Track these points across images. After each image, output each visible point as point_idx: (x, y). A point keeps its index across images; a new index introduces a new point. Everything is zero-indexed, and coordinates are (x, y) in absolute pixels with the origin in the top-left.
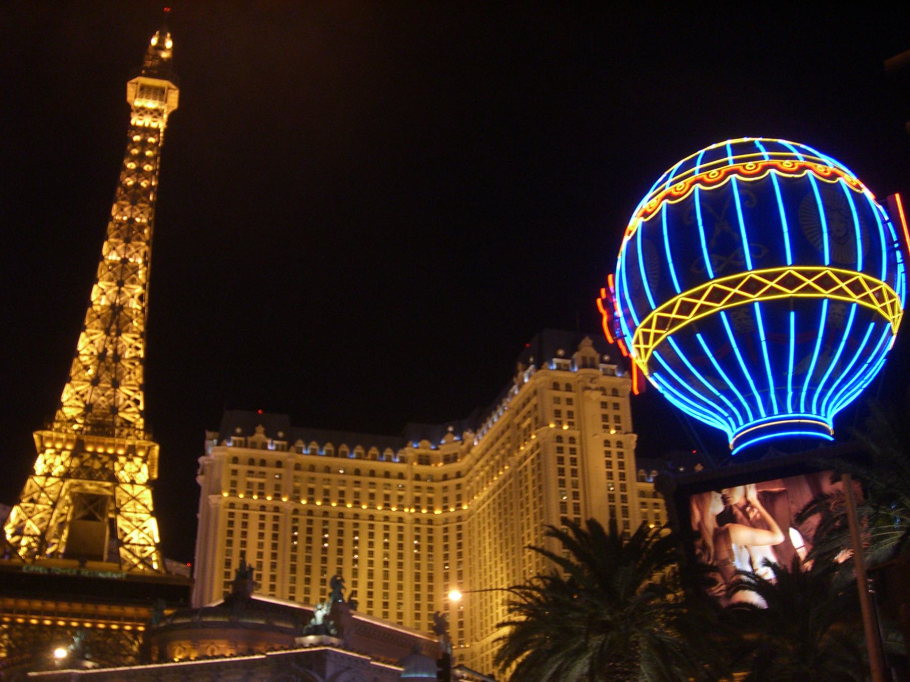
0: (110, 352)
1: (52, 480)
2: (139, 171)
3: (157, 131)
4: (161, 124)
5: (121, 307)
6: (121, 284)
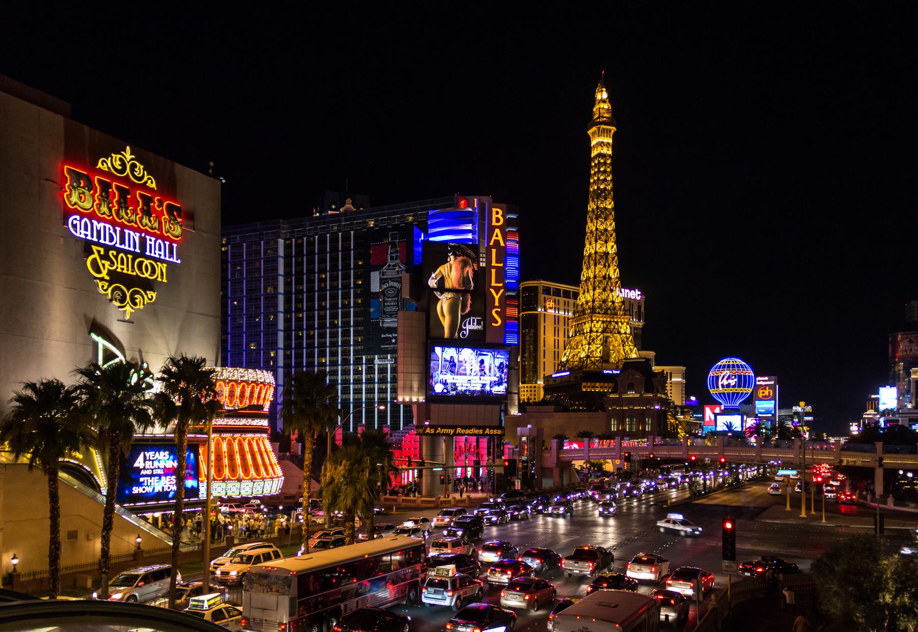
2: (605, 180)
3: (609, 156)
4: (610, 152)
6: (606, 242)
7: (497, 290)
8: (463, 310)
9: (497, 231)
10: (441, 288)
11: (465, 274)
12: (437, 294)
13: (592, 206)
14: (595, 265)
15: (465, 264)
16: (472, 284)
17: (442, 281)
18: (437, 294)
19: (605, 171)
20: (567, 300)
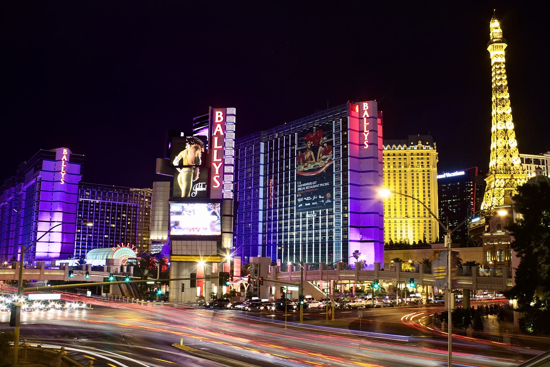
0: (507, 146)
1: (501, 189)
2: (501, 79)
3: (504, 63)
4: (503, 60)
5: (507, 130)
6: (505, 122)
7: (217, 163)
8: (194, 179)
9: (219, 126)
10: (181, 166)
11: (196, 156)
12: (178, 169)
13: (494, 98)
14: (497, 139)
15: (196, 148)
16: (201, 161)
17: (181, 161)
18: (178, 169)
19: (501, 74)
20: (529, 165)
